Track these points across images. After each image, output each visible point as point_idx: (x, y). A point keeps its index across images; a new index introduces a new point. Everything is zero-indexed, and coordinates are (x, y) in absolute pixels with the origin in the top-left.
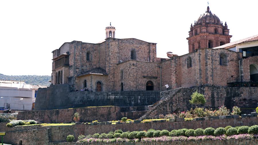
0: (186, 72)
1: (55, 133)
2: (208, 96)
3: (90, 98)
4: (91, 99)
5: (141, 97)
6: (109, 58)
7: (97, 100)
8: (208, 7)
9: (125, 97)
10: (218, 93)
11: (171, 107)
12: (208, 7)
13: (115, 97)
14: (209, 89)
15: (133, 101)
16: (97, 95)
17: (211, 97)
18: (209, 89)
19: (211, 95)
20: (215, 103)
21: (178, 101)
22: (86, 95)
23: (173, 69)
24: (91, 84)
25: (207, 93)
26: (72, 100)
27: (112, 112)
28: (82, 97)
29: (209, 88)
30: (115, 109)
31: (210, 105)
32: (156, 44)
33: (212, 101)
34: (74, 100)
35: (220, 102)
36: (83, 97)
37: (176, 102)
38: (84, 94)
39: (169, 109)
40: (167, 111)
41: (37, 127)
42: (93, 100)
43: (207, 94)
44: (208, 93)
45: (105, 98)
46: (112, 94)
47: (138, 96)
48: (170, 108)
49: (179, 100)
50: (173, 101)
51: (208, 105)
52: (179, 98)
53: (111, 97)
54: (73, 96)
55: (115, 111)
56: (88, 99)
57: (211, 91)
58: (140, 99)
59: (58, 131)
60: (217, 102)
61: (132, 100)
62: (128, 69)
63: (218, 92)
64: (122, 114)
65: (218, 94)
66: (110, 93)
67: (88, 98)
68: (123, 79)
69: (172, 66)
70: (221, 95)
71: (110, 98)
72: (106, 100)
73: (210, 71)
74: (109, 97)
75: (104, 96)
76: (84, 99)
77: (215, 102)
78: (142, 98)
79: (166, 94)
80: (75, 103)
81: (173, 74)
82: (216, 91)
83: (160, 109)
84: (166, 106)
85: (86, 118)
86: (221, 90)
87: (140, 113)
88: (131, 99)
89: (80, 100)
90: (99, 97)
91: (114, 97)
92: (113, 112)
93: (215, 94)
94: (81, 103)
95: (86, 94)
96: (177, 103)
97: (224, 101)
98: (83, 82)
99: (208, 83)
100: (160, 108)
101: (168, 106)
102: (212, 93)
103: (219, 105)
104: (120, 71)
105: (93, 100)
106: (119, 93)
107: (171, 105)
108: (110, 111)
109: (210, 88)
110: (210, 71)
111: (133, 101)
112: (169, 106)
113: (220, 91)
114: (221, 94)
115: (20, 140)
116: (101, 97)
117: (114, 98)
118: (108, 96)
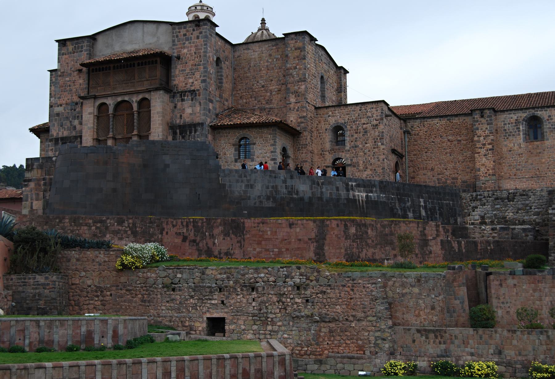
0: (520, 151)
1: (403, 295)
3: (297, 191)
4: (301, 195)
5: (425, 202)
6: (306, 87)
7: (321, 199)
8: (263, 20)
9: (392, 199)
12: (263, 20)
13: (367, 196)
15: (410, 211)
16: (318, 184)
22: (285, 181)
23: (482, 138)
24: (272, 152)
26: (237, 193)
27: (430, 238)
28: (273, 187)
30: (437, 231)
32: (346, 72)
34: (245, 192)
36: (275, 188)
38: (275, 177)
41: (301, 275)
42: (307, 200)
45: (340, 195)
46: (358, 186)
47: (419, 198)
53: (358, 195)
54: (237, 181)
55: (438, 235)
56: (290, 193)
58: (425, 208)
59: (416, 290)
61: (408, 207)
62: (375, 122)
64: (453, 245)
66: (354, 184)
67: (292, 190)
68: (347, 148)
69: (479, 132)
71: (354, 196)
72: (345, 202)
74: (351, 192)
75: (338, 189)
76: (277, 191)
78: (429, 206)
79: (497, 199)
80: (251, 203)
81: (483, 151)
85: (365, 251)
87: (492, 245)
88: (405, 204)
89: (264, 194)
90: (324, 190)
91: (364, 195)
92: (434, 238)
94: (270, 204)
95: (282, 178)
98: (234, 145)
104: (329, 127)
105: (307, 200)
106: (374, 186)
108: (425, 235)
111: (410, 211)
115: (208, 315)
116: (330, 193)
117: (364, 199)
118: (348, 190)
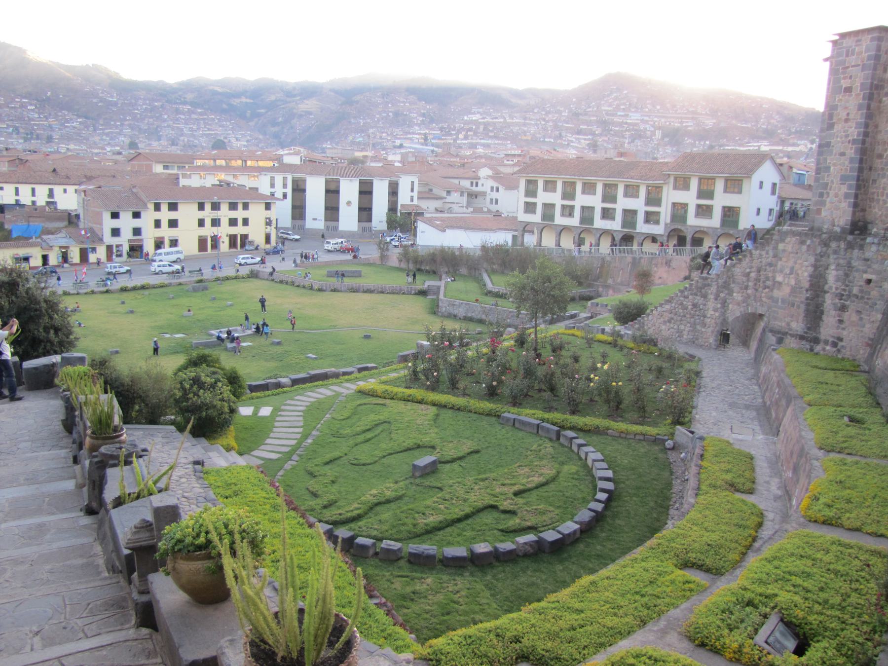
2: (793, 282)
10: (848, 270)
11: (724, 303)
14: (804, 248)
17: (806, 285)
18: (804, 248)
19: (811, 276)
20: (824, 317)
21: (755, 284)
25: (791, 264)
29: (803, 243)
31: (794, 325)
33: (808, 305)
35: (854, 317)
37: (746, 288)
39: (715, 310)
40: (705, 316)
43: (792, 269)
44: (797, 267)
48: (719, 306)
49: (757, 280)
50: (734, 282)
51: (788, 324)
52: (759, 271)
57: (812, 259)
60: (833, 312)
63: (849, 266)
65: (847, 275)
70: (869, 281)
73: (843, 154)
77: (822, 312)
82: (841, 261)
83: (682, 304)
84: (705, 296)
86: (868, 255)
93: (832, 276)
96: (749, 291)
97: (879, 316)
99: (823, 214)
100: (682, 299)
101: (712, 297)
102: (815, 267)
103: (845, 333)
107: (722, 295)
109: (808, 242)
110: (843, 154)
112: (716, 299)
113: (866, 260)
114: (866, 276)
